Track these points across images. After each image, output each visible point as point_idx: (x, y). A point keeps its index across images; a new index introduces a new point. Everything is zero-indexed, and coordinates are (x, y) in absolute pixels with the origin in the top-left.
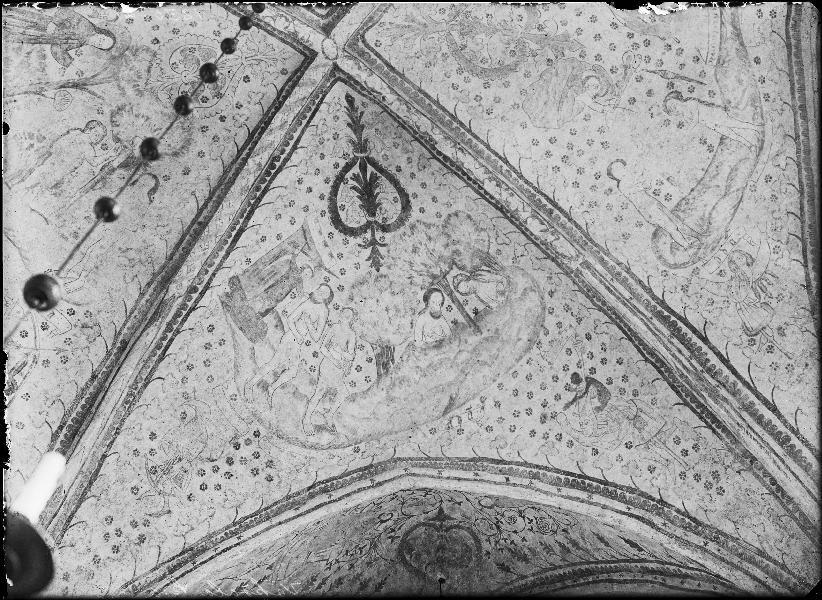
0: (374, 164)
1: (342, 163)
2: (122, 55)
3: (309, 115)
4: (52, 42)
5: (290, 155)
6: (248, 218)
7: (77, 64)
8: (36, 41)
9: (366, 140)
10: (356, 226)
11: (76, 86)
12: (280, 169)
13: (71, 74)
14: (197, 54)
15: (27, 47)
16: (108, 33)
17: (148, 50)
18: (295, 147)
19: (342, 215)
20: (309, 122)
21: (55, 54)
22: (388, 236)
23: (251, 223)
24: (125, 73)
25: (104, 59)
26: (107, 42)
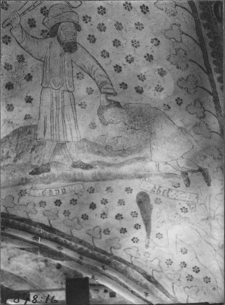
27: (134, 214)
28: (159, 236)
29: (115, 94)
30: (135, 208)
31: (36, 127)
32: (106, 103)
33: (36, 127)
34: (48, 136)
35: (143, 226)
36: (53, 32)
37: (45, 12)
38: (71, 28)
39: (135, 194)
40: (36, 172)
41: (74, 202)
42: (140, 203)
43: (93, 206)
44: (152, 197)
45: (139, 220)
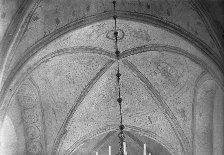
0: (113, 39)
1: (120, 41)
2: (157, 63)
3: (125, 52)
4: (167, 72)
5: (130, 49)
6: (141, 47)
7: (165, 66)
8: (169, 74)
9: (114, 43)
10: (120, 31)
11: (167, 63)
12: (133, 49)
13: (167, 65)
14: (144, 59)
15: (171, 74)
16: (158, 68)
17: (153, 62)
18: (129, 50)
19: (122, 33)
20: (125, 51)
21: (168, 70)
22: (112, 29)
23: (141, 46)
24: (158, 60)
25: (161, 64)
26: (159, 67)
27: (149, 121)
28: (154, 124)
29: (140, 100)
30: (148, 120)
31: (129, 108)
32: (139, 102)
33: (129, 108)
34: (131, 110)
35: (151, 123)
36: (128, 93)
37: (127, 90)
38: (131, 91)
39: (148, 117)
40: (130, 116)
41: (138, 121)
42: (149, 119)
43: (141, 121)
44: (151, 117)
45: (150, 122)
